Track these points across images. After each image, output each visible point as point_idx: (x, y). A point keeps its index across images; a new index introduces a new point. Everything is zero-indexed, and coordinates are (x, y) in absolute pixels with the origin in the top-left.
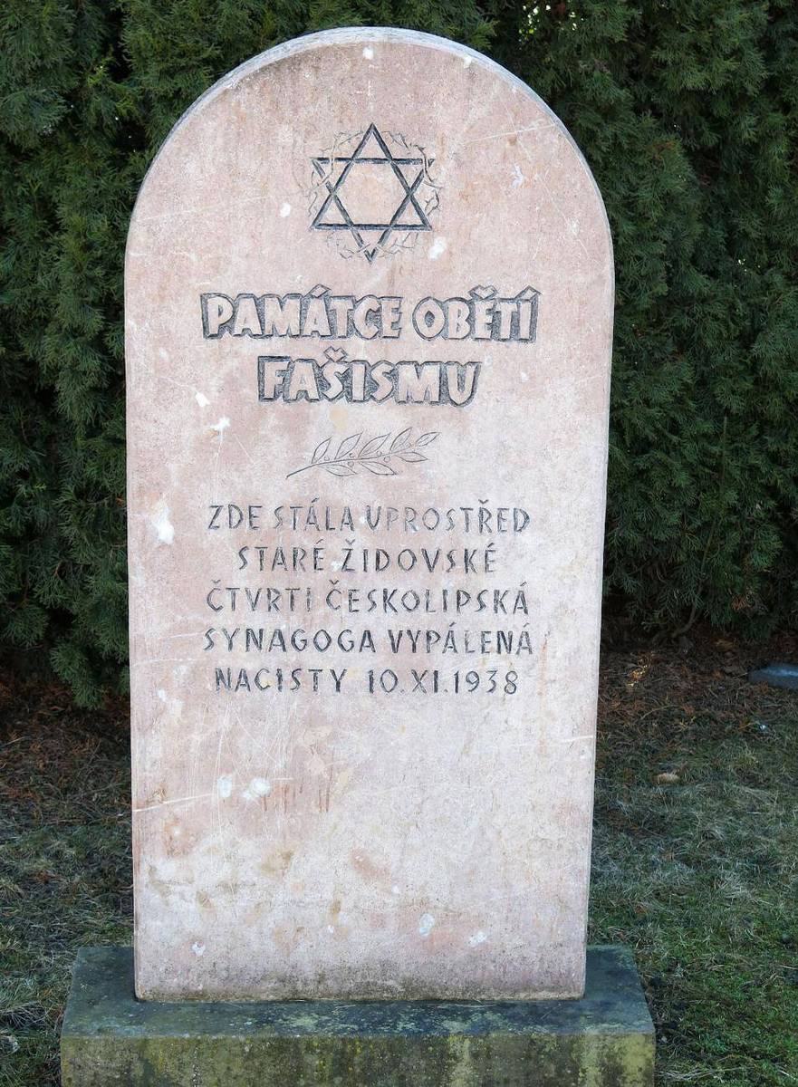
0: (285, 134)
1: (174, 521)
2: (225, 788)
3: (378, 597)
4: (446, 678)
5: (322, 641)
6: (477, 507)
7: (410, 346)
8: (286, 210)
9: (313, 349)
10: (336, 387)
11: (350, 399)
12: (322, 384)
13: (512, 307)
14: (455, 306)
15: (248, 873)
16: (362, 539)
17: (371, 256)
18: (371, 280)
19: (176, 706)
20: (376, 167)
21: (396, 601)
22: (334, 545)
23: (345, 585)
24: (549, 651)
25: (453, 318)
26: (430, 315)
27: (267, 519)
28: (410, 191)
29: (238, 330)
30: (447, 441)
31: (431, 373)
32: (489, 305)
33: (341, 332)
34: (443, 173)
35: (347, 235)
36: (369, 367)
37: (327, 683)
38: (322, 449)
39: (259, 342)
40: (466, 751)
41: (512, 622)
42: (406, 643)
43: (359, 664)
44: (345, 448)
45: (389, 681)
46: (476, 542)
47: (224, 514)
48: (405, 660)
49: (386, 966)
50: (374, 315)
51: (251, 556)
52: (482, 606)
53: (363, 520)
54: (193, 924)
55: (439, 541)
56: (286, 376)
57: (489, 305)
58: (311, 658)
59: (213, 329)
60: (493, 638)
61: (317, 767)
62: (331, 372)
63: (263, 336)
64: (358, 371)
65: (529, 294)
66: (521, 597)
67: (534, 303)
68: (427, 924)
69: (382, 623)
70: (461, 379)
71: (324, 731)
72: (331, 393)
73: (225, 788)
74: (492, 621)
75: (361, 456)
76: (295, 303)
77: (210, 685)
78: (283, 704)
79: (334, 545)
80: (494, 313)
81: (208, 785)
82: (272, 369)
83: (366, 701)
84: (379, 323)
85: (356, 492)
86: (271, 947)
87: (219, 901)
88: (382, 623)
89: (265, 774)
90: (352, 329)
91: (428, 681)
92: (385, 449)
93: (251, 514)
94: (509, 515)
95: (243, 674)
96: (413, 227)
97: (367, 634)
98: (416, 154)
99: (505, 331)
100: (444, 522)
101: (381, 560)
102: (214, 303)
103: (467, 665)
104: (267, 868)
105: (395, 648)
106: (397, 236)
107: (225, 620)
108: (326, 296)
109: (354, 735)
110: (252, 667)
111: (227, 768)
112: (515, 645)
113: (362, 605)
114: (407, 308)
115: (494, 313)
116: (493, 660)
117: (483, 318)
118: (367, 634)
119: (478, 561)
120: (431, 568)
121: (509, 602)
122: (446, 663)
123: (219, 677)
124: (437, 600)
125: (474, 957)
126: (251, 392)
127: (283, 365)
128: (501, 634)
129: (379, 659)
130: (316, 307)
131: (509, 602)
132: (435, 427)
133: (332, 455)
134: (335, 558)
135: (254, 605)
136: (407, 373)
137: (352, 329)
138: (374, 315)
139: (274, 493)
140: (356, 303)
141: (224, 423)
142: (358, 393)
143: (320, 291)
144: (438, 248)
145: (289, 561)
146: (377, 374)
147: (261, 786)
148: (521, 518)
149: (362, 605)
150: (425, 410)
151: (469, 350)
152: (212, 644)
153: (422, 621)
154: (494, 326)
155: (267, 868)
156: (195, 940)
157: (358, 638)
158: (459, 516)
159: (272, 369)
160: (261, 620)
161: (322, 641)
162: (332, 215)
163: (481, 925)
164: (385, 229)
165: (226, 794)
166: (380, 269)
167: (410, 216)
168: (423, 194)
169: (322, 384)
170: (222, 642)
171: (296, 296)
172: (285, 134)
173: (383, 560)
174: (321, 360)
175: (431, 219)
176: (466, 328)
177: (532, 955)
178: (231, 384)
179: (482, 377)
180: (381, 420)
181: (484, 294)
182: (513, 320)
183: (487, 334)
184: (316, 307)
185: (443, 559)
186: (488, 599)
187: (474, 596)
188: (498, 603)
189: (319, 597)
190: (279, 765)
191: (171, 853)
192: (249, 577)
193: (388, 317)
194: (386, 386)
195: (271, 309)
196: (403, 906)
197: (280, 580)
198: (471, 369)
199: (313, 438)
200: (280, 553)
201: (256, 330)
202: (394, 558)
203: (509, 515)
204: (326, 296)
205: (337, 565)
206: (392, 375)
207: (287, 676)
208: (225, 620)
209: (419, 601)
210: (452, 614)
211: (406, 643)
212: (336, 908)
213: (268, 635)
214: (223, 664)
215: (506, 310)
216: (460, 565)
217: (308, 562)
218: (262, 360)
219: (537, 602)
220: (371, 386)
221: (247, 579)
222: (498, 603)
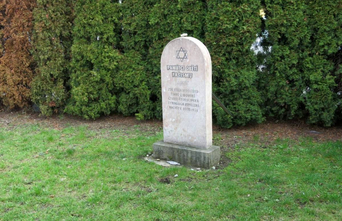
1: (165, 90)
2: (171, 119)
4: (191, 109)
8: (174, 56)
9: (177, 71)
12: (178, 75)
14: (190, 67)
15: (173, 130)
16: (182, 93)
18: (182, 64)
19: (166, 110)
21: (186, 100)
22: (180, 93)
23: (181, 98)
26: (187, 68)
27: (173, 90)
28: (185, 54)
31: (188, 74)
34: (188, 52)
36: (182, 74)
40: (193, 118)
41: (197, 103)
43: (183, 107)
46: (193, 94)
48: (187, 107)
50: (182, 68)
51: (172, 94)
54: (168, 135)
55: (190, 93)
58: (178, 106)
62: (179, 74)
66: (198, 100)
68: (190, 138)
69: (185, 102)
75: (182, 83)
78: (176, 110)
79: (180, 93)
80: (194, 68)
82: (173, 73)
85: (181, 87)
87: (171, 132)
88: (185, 102)
89: (174, 118)
90: (180, 70)
91: (189, 109)
101: (184, 95)
102: (168, 66)
103: (193, 108)
104: (175, 129)
105: (186, 105)
106: (184, 59)
107: (170, 101)
108: (178, 66)
110: (173, 106)
111: (171, 117)
114: (185, 67)
115: (194, 68)
116: (195, 108)
119: (193, 96)
121: (197, 101)
122: (191, 108)
124: (190, 100)
125: (195, 142)
126: (172, 76)
130: (177, 67)
131: (197, 101)
136: (186, 74)
137: (180, 70)
138: (182, 68)
139: (174, 87)
147: (174, 120)
150: (187, 78)
151: (191, 72)
153: (188, 102)
154: (194, 69)
155: (175, 129)
156: (169, 136)
157: (182, 104)
159: (173, 73)
160: (173, 101)
162: (178, 57)
164: (183, 58)
167: (185, 57)
169: (178, 75)
170: (170, 103)
177: (201, 143)
178: (170, 75)
180: (183, 79)
184: (177, 67)
186: (194, 100)
188: (195, 101)
191: (166, 126)
193: (184, 68)
194: (184, 76)
196: (188, 135)
197: (175, 97)
200: (175, 94)
204: (178, 66)
206: (184, 74)
209: (188, 100)
210: (191, 102)
211: (187, 105)
212: (181, 135)
215: (195, 67)
218: (172, 73)
220: (182, 76)
221: (172, 96)
222: (195, 101)
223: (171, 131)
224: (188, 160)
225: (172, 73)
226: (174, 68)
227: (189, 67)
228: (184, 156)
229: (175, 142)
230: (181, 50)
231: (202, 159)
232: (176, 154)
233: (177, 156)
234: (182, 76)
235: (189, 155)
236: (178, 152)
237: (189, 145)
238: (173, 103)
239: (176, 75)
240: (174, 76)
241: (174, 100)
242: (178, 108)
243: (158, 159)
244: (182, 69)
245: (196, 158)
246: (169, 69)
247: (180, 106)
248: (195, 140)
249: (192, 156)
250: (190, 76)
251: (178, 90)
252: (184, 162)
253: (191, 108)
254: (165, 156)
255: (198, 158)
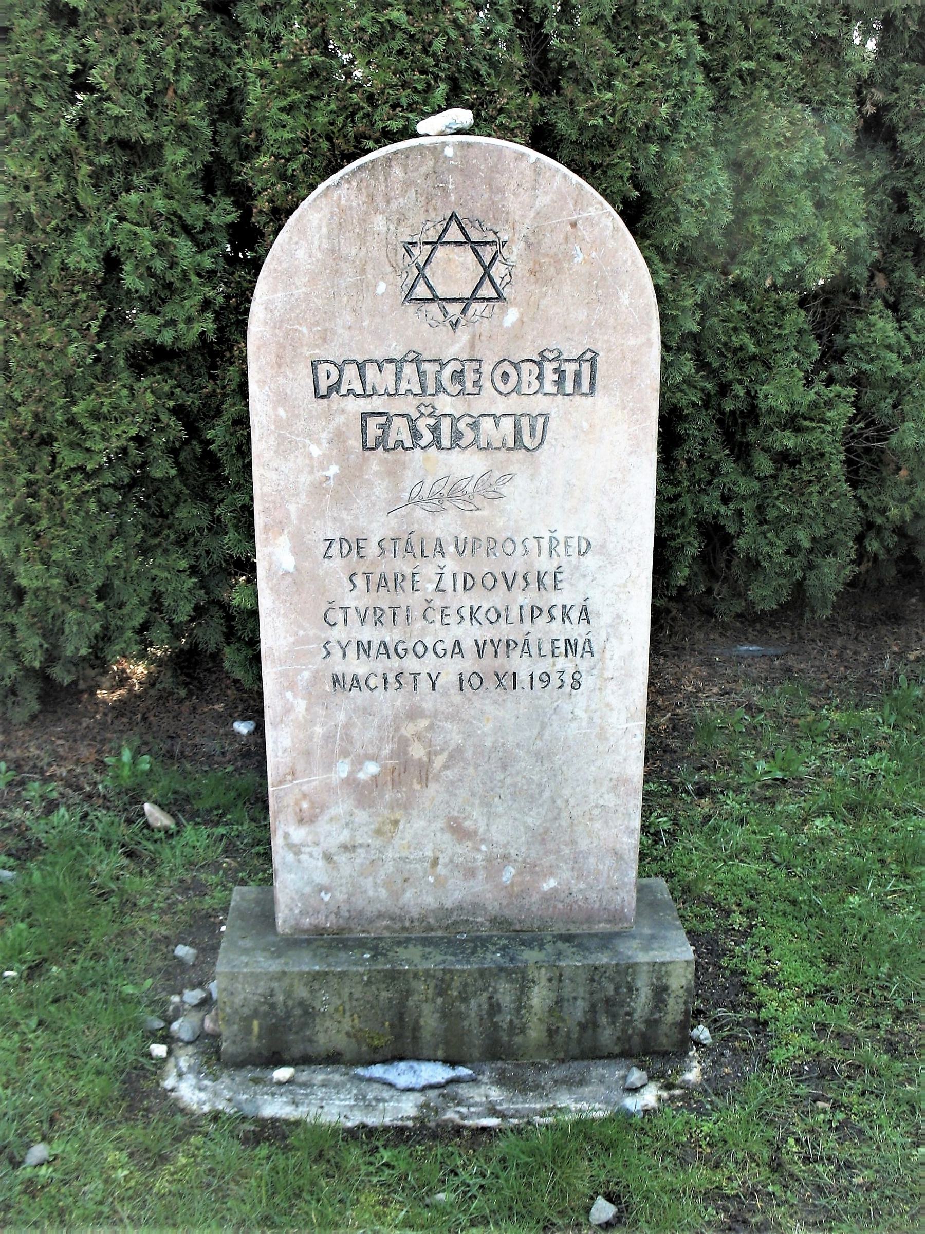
0: (379, 223)
1: (295, 552)
3: (466, 613)
4: (523, 677)
5: (420, 649)
6: (547, 535)
7: (489, 401)
8: (382, 287)
9: (408, 405)
10: (428, 437)
11: (439, 448)
12: (416, 434)
13: (573, 367)
14: (526, 367)
16: (451, 565)
17: (455, 325)
18: (455, 346)
19: (301, 705)
20: (458, 249)
21: (480, 616)
22: (428, 570)
23: (438, 603)
24: (608, 655)
25: (525, 377)
26: (505, 375)
27: (372, 550)
28: (487, 269)
29: (343, 391)
30: (521, 481)
31: (507, 424)
32: (555, 365)
33: (431, 390)
34: (515, 253)
35: (434, 308)
36: (455, 420)
37: (424, 684)
38: (417, 490)
39: (362, 401)
40: (540, 735)
41: (577, 631)
42: (489, 649)
43: (450, 669)
44: (436, 489)
45: (476, 681)
47: (336, 546)
49: (476, 907)
50: (458, 376)
51: (360, 581)
52: (553, 618)
53: (452, 549)
54: (321, 878)
55: (516, 565)
56: (384, 428)
57: (555, 365)
58: (411, 664)
59: (323, 391)
60: (561, 644)
61: (417, 752)
63: (365, 395)
64: (446, 424)
65: (589, 355)
66: (585, 609)
67: (593, 361)
68: (509, 874)
70: (533, 428)
71: (423, 723)
72: (423, 443)
73: (343, 769)
74: (560, 630)
75: (448, 495)
76: (391, 367)
77: (328, 687)
78: (389, 702)
79: (428, 570)
80: (560, 372)
81: (329, 766)
83: (457, 698)
84: (462, 383)
85: (445, 525)
86: (383, 893)
87: (342, 859)
88: (469, 634)
89: (374, 758)
90: (440, 388)
91: (507, 681)
92: (469, 489)
93: (358, 546)
94: (574, 543)
95: (355, 678)
96: (489, 300)
97: (457, 643)
98: (491, 237)
99: (569, 386)
100: (520, 549)
101: (468, 582)
102: (323, 369)
105: (480, 654)
106: (476, 307)
107: (338, 634)
108: (417, 361)
109: (448, 726)
111: (345, 753)
112: (579, 649)
113: (453, 619)
114: (486, 368)
115: (560, 372)
116: (561, 663)
117: (550, 376)
118: (457, 643)
119: (548, 581)
120: (509, 588)
121: (574, 615)
122: (522, 665)
123: (336, 681)
124: (514, 614)
125: (548, 898)
126: (355, 443)
127: (382, 420)
128: (567, 641)
129: (468, 664)
130: (409, 370)
131: (574, 615)
132: (512, 469)
133: (425, 494)
134: (430, 581)
135: (363, 621)
136: (487, 424)
137: (440, 388)
138: (458, 376)
139: (378, 528)
140: (443, 365)
141: (334, 470)
142: (446, 443)
143: (412, 356)
144: (512, 316)
145: (391, 584)
146: (462, 425)
147: (372, 768)
148: (584, 545)
149: (453, 619)
150: (502, 455)
151: (540, 404)
152: (329, 653)
153: (503, 631)
154: (560, 382)
155: (379, 832)
156: (321, 888)
157: (449, 645)
158: (532, 544)
159: (372, 423)
160: (368, 633)
161: (420, 649)
162: (421, 291)
163: (552, 874)
164: (467, 302)
165: (344, 775)
166: (463, 335)
167: (488, 291)
168: (498, 271)
169: (416, 434)
171: (390, 361)
172: (379, 223)
173: (470, 582)
174: (414, 414)
175: (505, 293)
176: (536, 385)
177: (593, 896)
178: (339, 437)
179: (551, 425)
180: (465, 464)
181: (551, 356)
182: (578, 374)
183: (554, 390)
184: (409, 370)
185: (520, 579)
186: (557, 613)
187: (545, 610)
188: (566, 615)
189: (417, 613)
190: (386, 751)
191: (301, 821)
192: (357, 598)
193: (470, 377)
194: (469, 436)
195: (371, 372)
196: (489, 860)
197: (384, 600)
198: (541, 420)
199: (409, 480)
200: (383, 577)
201: (359, 390)
202: (478, 580)
203: (574, 543)
204: (417, 361)
205: (431, 587)
206: (475, 426)
207: (391, 679)
208: (338, 634)
210: (527, 626)
211: (489, 649)
212: (435, 862)
213: (375, 646)
214: (339, 670)
215: (570, 368)
216: (534, 586)
217: (407, 585)
218: (364, 416)
219: (598, 615)
220: (457, 436)
221: (356, 600)
222: (566, 615)
223: (346, 848)
224: (523, 1030)
225: (364, 416)
226: (383, 379)
227: (516, 366)
228: (494, 1008)
229: (380, 916)
230: (454, 234)
231: (642, 1001)
232: (427, 1008)
233: (430, 1022)
234: (457, 436)
235: (539, 997)
236: (442, 991)
237: (494, 921)
238: (363, 648)
239: (400, 430)
240: (381, 441)
241: (378, 622)
242: (407, 680)
243: (283, 1073)
244: (455, 388)
245: (593, 1008)
246: (334, 388)
247: (429, 663)
248: (550, 884)
249: (559, 1001)
250: (526, 437)
251: (410, 545)
252: (496, 1050)
253: (522, 665)
254: (331, 1034)
255: (608, 1001)
